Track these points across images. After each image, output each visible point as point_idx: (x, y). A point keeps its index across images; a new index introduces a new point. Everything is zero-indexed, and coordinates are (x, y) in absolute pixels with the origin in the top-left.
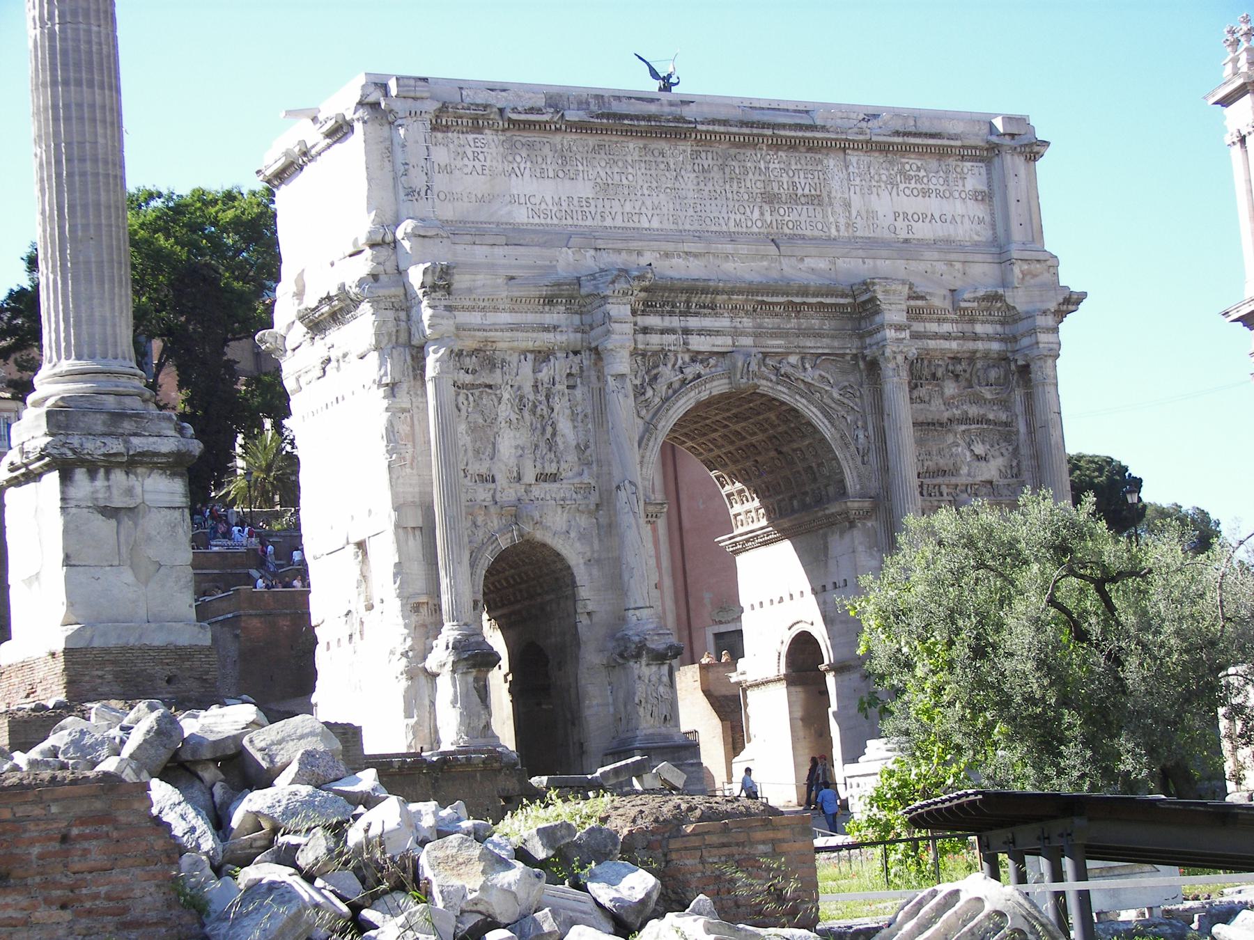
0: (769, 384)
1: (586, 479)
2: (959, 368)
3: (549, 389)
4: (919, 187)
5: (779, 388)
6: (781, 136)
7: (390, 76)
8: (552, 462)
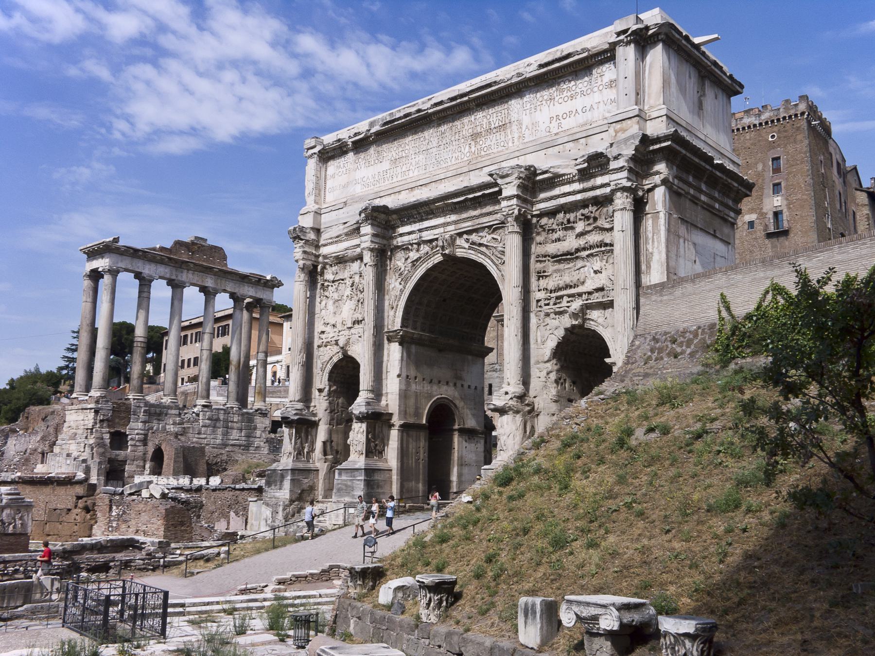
0: (464, 250)
2: (585, 211)
4: (569, 94)
5: (470, 251)
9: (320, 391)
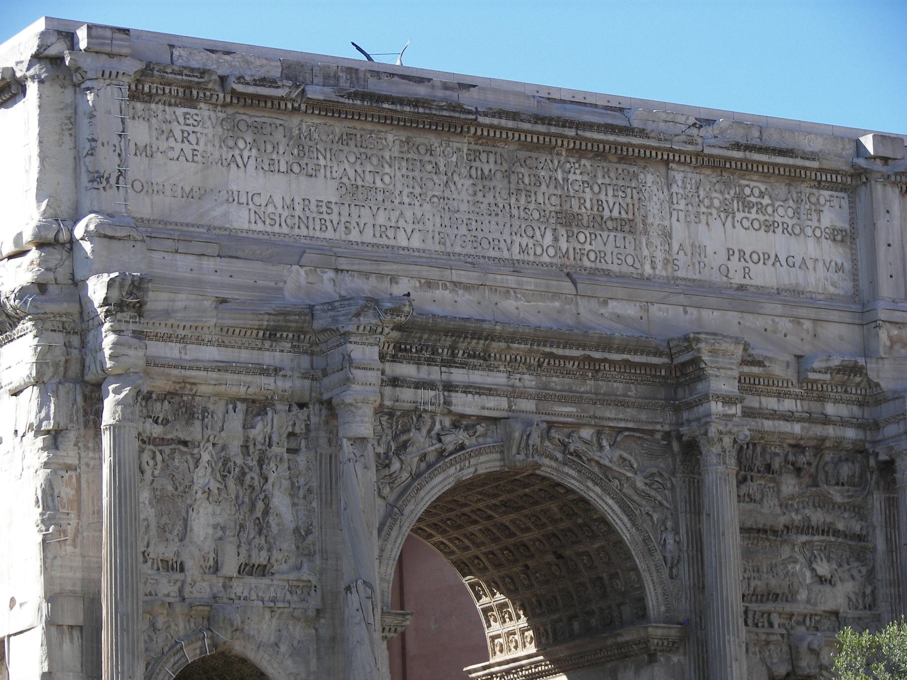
1: (305, 574)
2: (802, 459)
3: (263, 452)
4: (762, 218)
5: (566, 469)
6: (587, 140)
7: (79, 24)
8: (260, 549)
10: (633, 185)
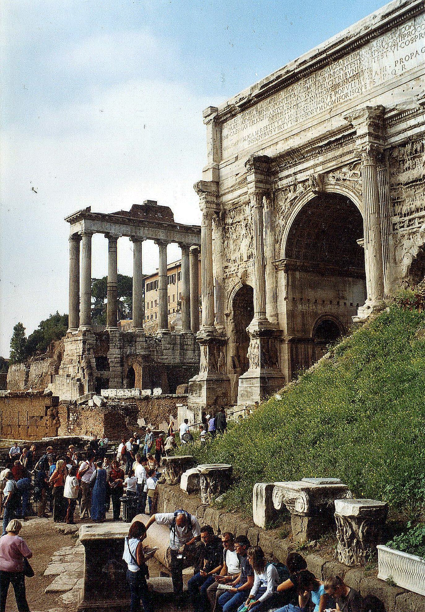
0: (332, 187)
4: (410, 38)
5: (336, 187)
9: (227, 315)
10: (357, 58)
